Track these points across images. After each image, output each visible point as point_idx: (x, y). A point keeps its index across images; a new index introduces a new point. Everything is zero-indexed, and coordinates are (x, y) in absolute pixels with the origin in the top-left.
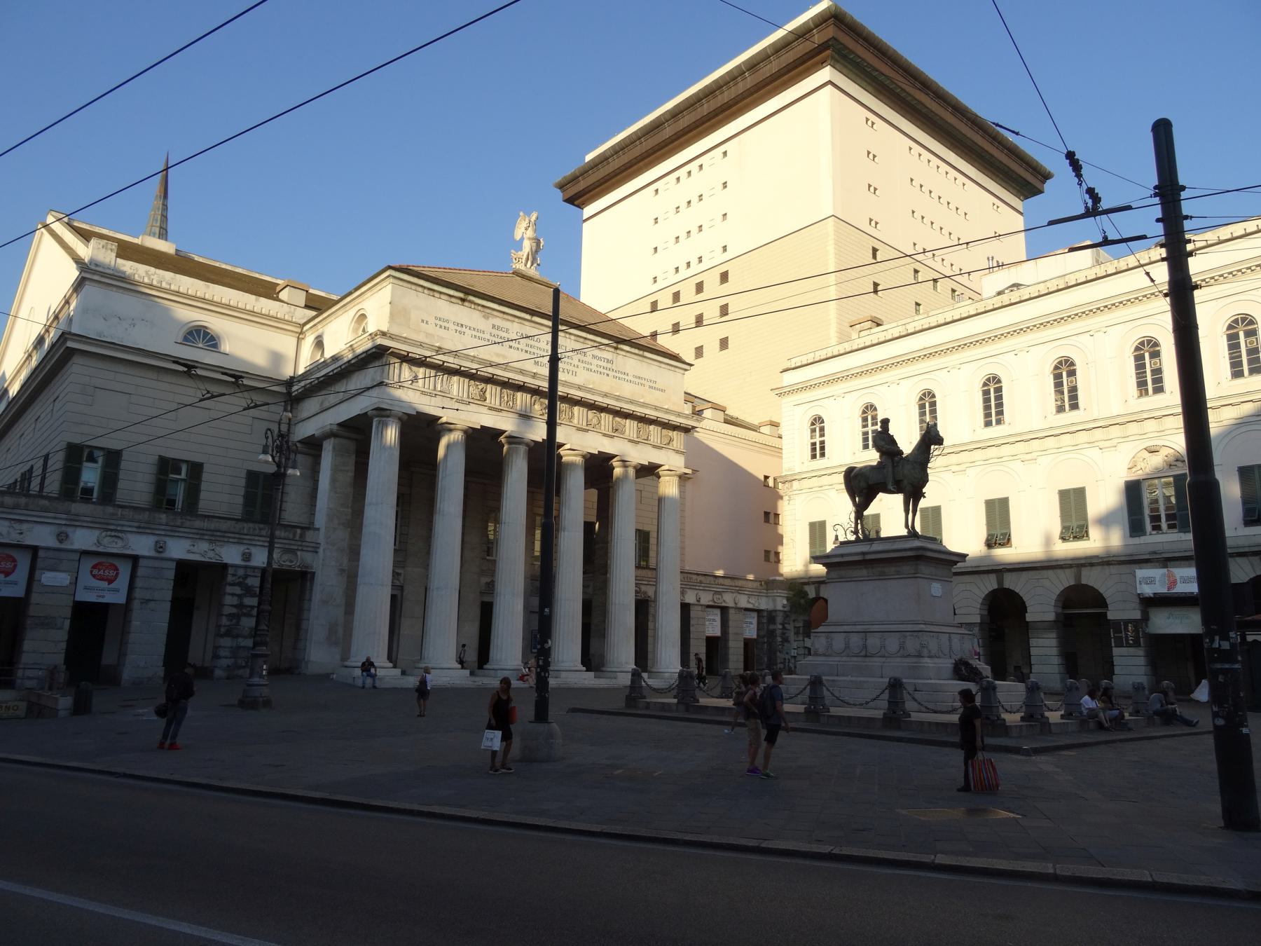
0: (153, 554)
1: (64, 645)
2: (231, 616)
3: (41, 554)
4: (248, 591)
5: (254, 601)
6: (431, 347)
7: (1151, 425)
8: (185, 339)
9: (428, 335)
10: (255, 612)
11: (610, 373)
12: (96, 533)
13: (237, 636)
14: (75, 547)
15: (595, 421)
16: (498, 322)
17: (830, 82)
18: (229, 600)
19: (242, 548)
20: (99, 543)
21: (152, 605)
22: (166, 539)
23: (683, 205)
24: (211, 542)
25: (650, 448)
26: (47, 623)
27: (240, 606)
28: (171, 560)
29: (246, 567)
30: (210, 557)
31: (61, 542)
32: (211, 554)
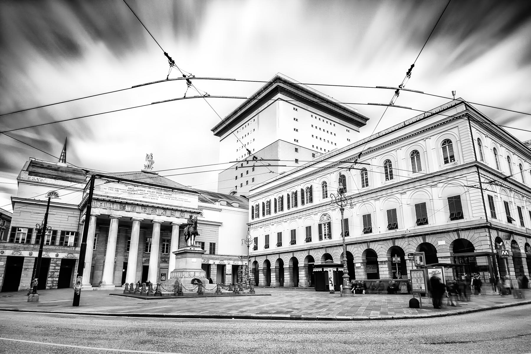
5: (59, 268)
7: (324, 208)
9: (106, 193)
10: (59, 271)
12: (12, 251)
14: (6, 255)
15: (164, 213)
16: (131, 187)
17: (279, 98)
18: (51, 268)
19: (56, 253)
23: (244, 136)
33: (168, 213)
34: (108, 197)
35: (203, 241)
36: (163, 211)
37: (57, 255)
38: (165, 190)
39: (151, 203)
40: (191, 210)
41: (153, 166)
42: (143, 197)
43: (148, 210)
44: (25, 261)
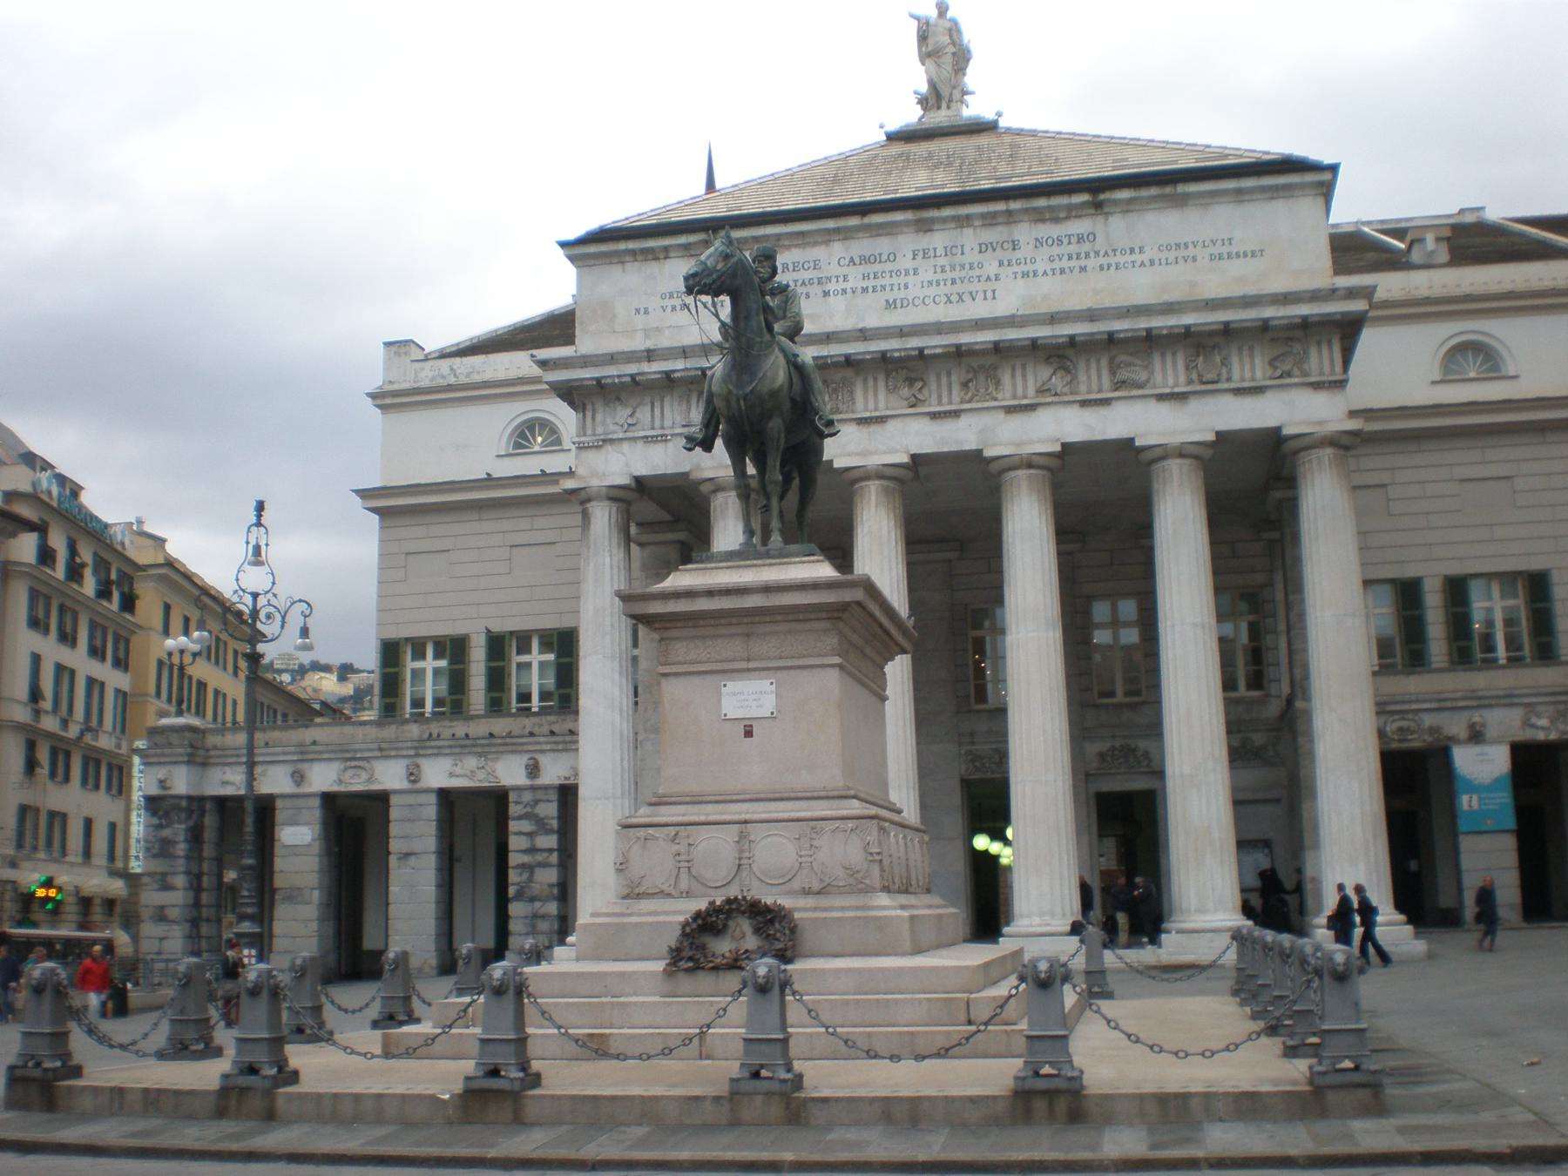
0: (405, 785)
1: (314, 926)
2: (523, 866)
3: (279, 804)
4: (542, 825)
6: (631, 357)
8: (518, 446)
9: (647, 332)
10: (554, 858)
11: (1091, 263)
12: (336, 766)
13: (532, 900)
15: (1058, 382)
20: (340, 782)
21: (412, 861)
22: (420, 761)
24: (480, 755)
25: (1229, 401)
26: (294, 896)
27: (532, 850)
28: (427, 791)
29: (533, 788)
30: (480, 781)
31: (298, 783)
32: (481, 775)
33: (1093, 376)
34: (650, 355)
35: (1536, 565)
36: (1045, 372)
37: (533, 770)
38: (1039, 217)
39: (939, 328)
40: (1269, 312)
41: (971, 78)
42: (890, 305)
43: (944, 391)
44: (394, 813)
